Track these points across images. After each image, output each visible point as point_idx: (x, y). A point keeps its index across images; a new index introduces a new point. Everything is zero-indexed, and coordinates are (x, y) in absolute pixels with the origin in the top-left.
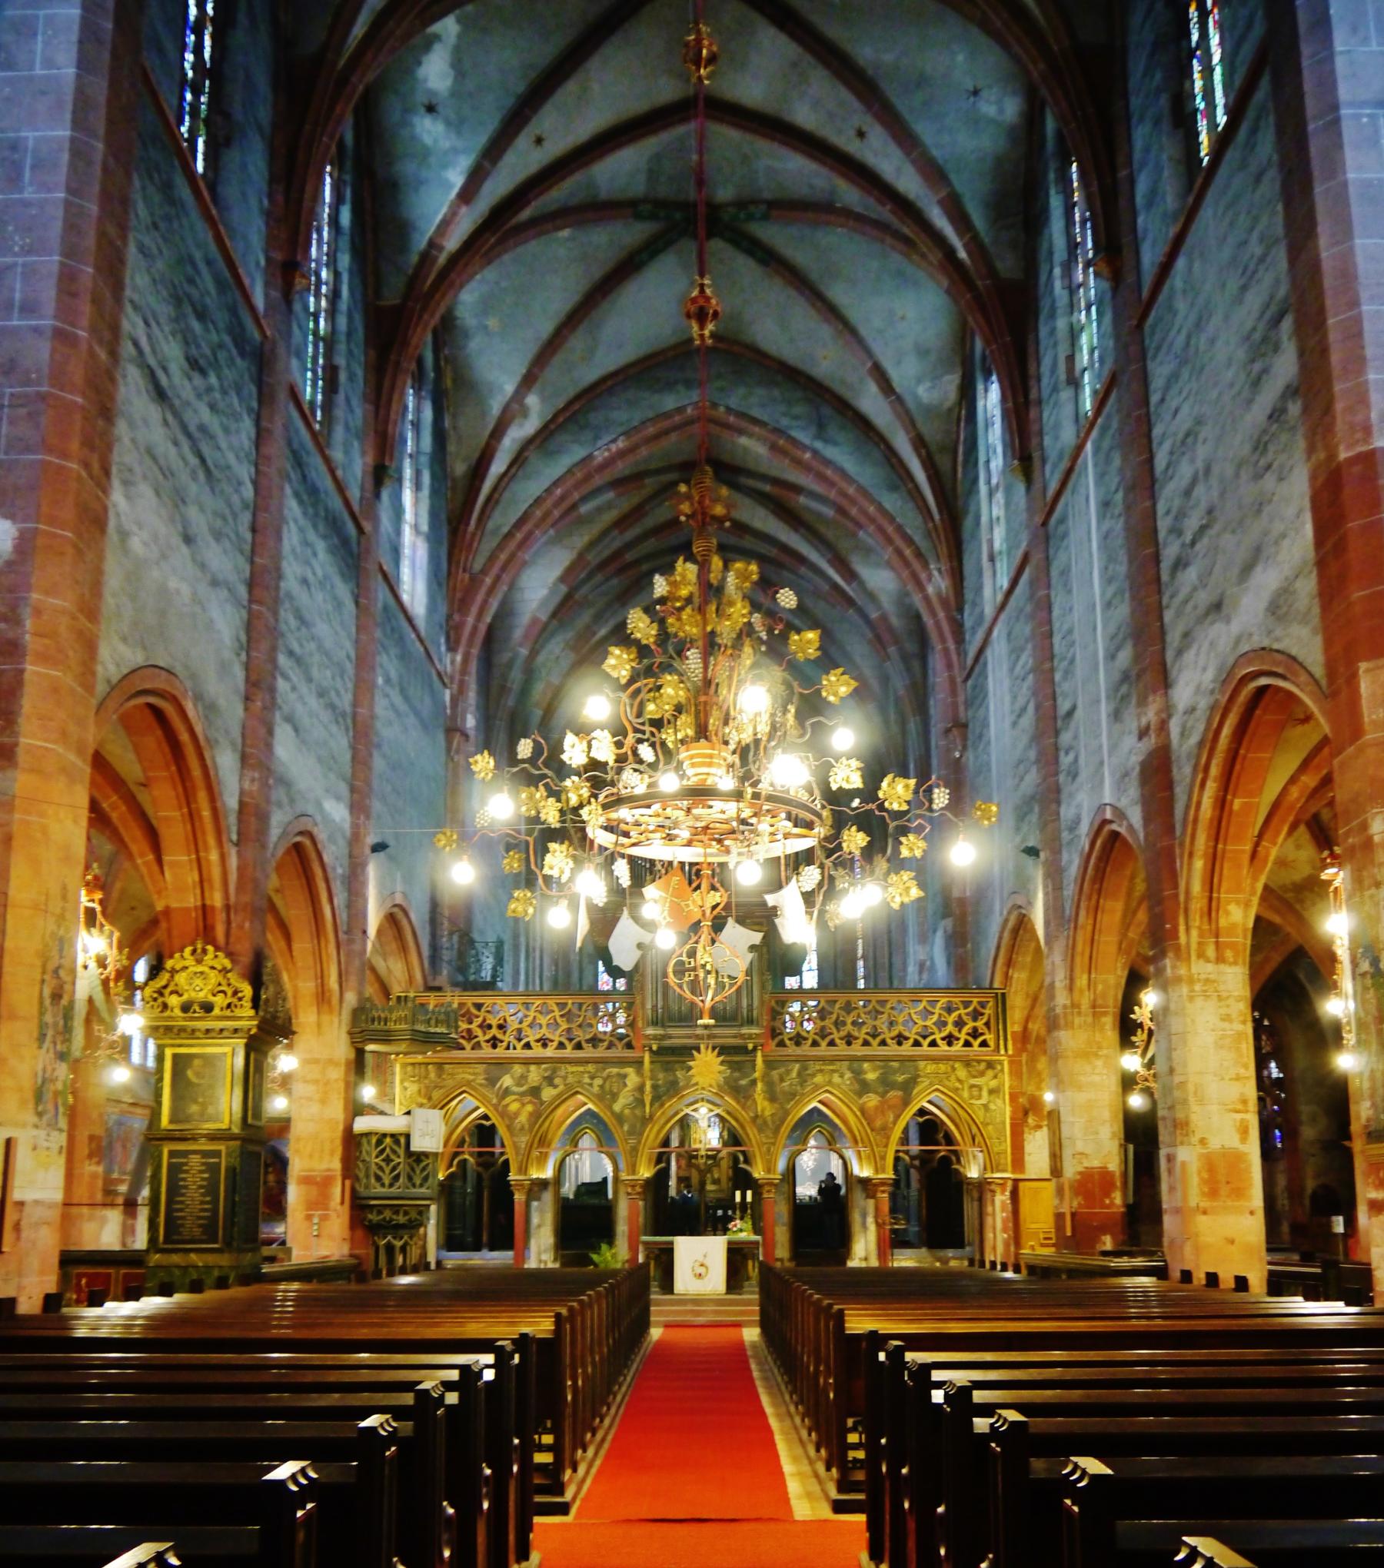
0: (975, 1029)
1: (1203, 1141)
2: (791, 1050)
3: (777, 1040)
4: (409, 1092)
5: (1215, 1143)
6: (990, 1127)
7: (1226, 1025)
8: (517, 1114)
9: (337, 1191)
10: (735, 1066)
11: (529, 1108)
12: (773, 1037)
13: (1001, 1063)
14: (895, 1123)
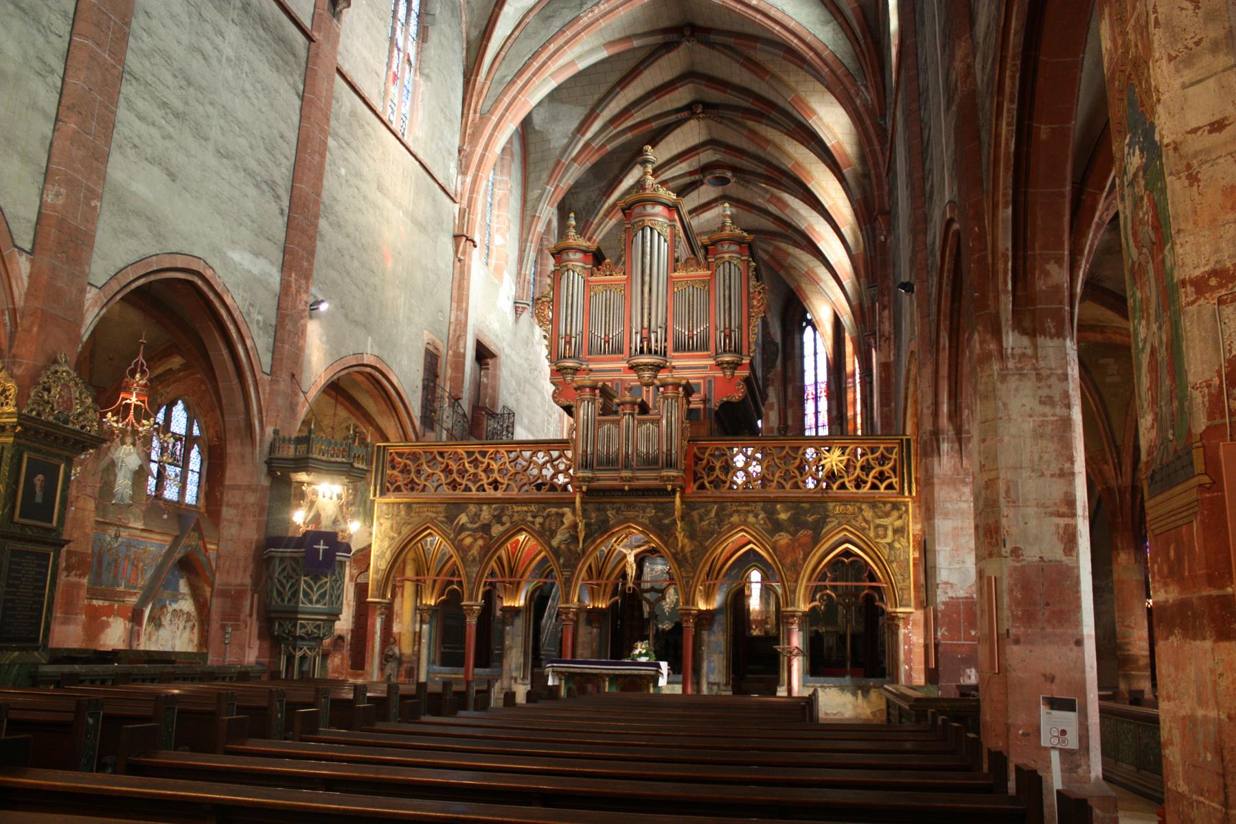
0: (881, 473)
1: (1016, 552)
2: (710, 491)
3: (697, 484)
4: (383, 528)
5: (1031, 554)
6: (894, 565)
7: (1047, 409)
8: (470, 547)
9: (247, 604)
10: (658, 507)
11: (480, 542)
12: (695, 482)
13: (906, 505)
14: (805, 559)
